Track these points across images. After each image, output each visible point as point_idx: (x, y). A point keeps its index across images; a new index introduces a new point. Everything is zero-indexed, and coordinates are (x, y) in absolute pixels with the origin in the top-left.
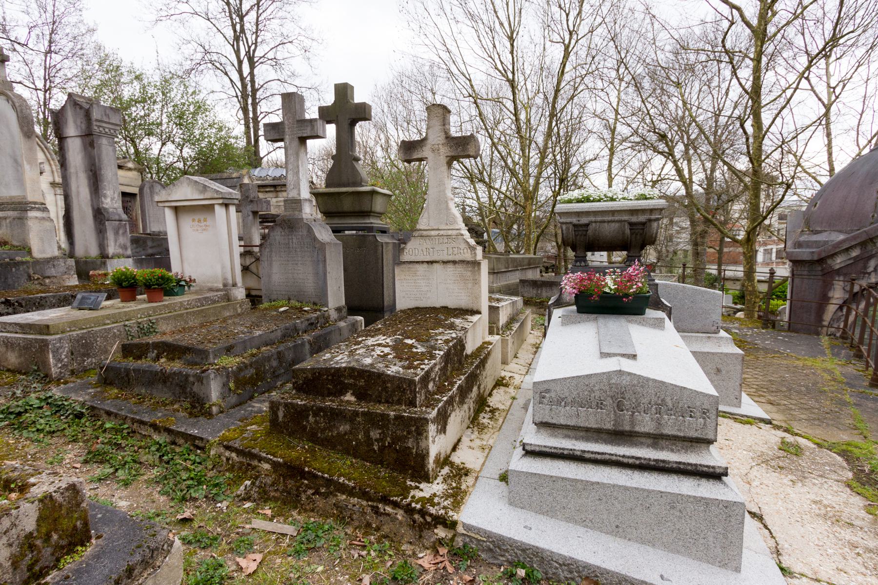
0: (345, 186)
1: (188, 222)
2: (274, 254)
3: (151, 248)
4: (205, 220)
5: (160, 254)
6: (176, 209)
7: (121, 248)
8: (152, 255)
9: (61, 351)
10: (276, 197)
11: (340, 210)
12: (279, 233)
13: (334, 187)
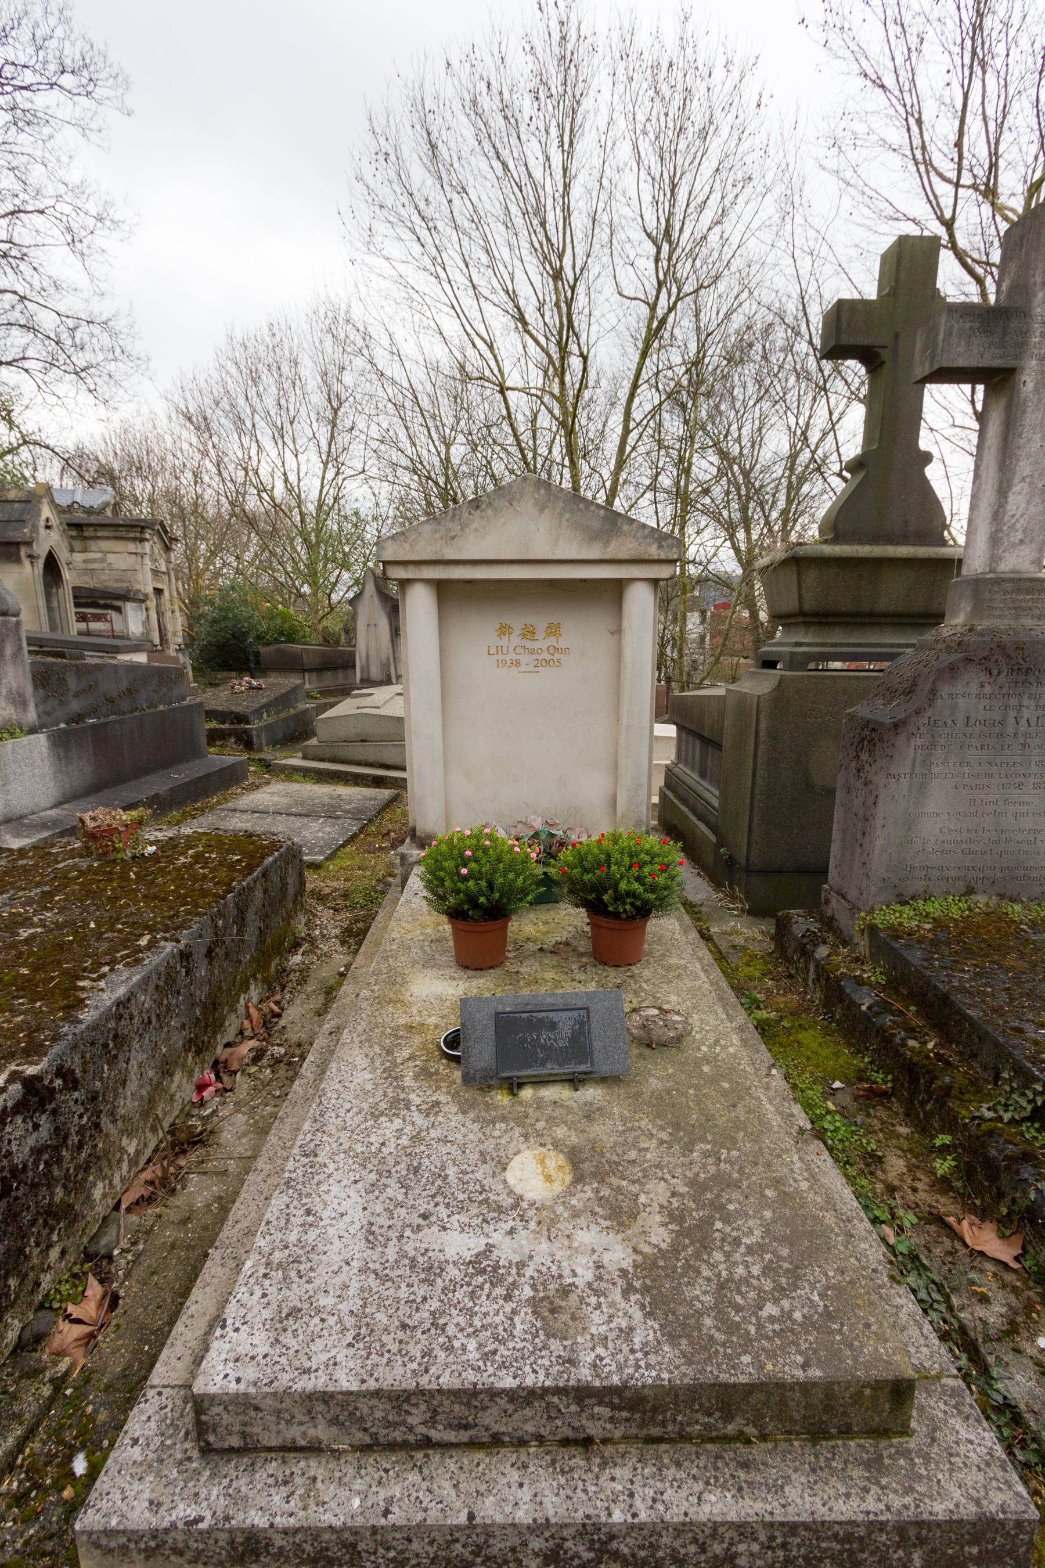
0: (903, 539)
1: (480, 638)
2: (939, 753)
3: (76, 696)
4: (553, 630)
5: (93, 712)
6: (443, 589)
7: (14, 702)
8: (79, 718)
9: (947, 1476)
10: (84, 550)
11: (865, 608)
12: (974, 688)
13: (861, 542)
